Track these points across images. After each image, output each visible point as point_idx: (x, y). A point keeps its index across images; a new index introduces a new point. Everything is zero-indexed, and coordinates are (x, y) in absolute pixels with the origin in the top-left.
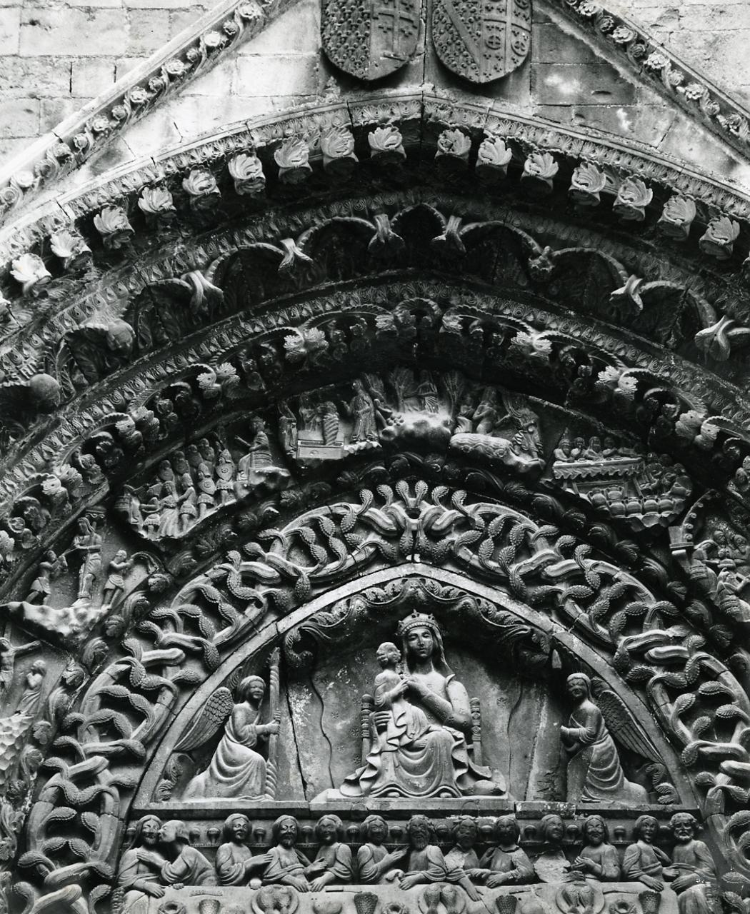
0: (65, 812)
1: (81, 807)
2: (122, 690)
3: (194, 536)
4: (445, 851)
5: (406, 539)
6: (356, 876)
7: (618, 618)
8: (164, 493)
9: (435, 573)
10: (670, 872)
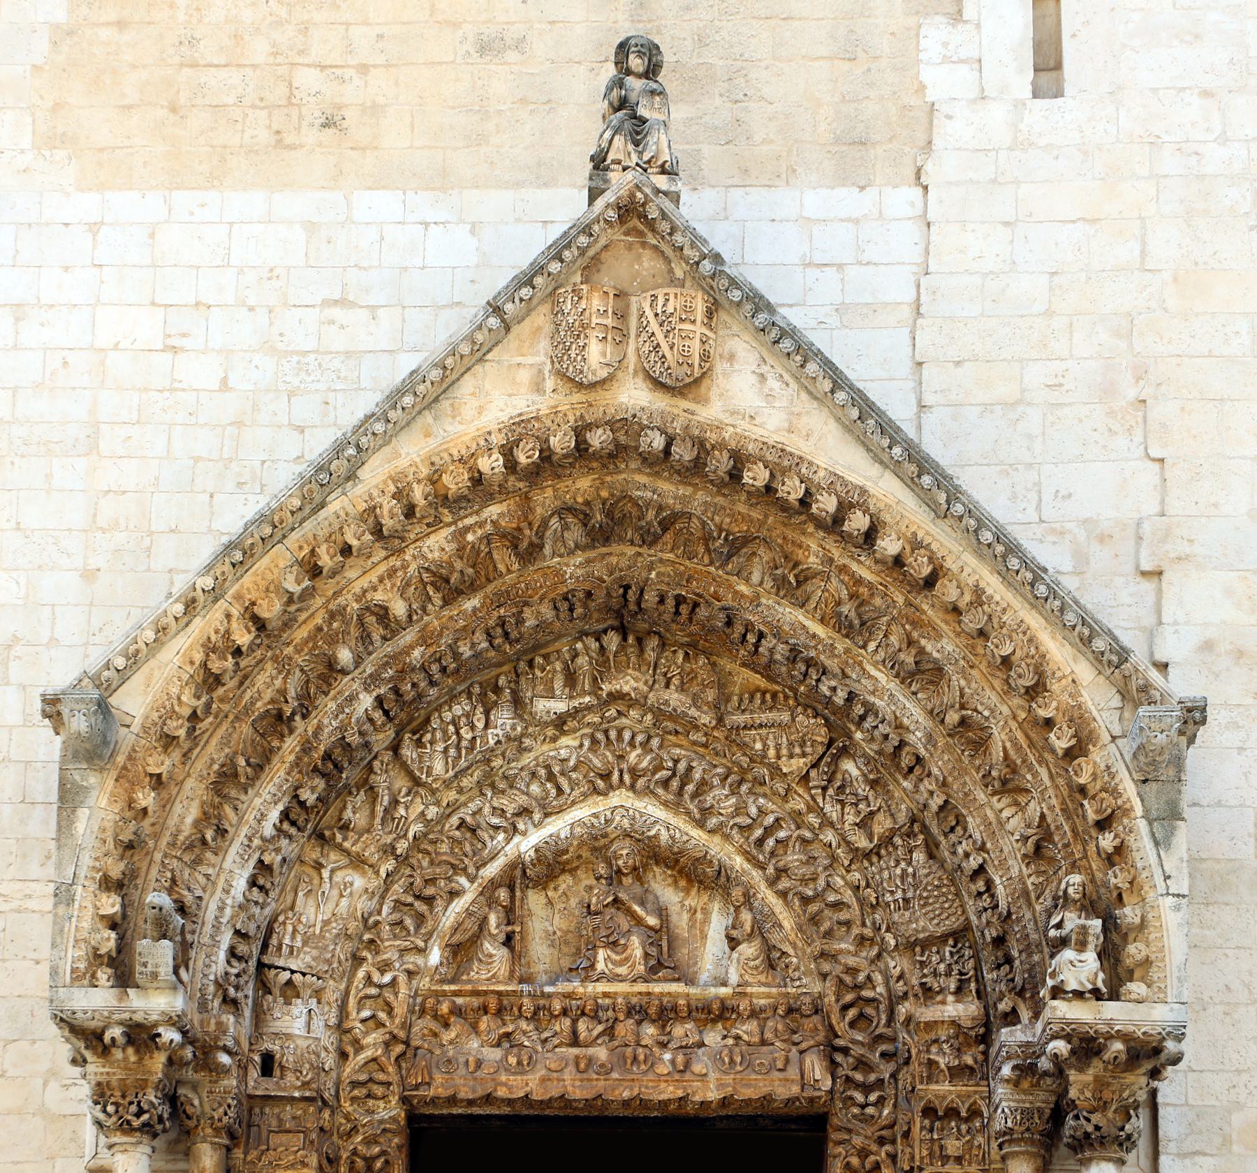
0: (373, 991)
1: (380, 987)
2: (410, 899)
4: (639, 1023)
5: (615, 777)
6: (575, 1041)
8: (432, 743)
10: (796, 1038)
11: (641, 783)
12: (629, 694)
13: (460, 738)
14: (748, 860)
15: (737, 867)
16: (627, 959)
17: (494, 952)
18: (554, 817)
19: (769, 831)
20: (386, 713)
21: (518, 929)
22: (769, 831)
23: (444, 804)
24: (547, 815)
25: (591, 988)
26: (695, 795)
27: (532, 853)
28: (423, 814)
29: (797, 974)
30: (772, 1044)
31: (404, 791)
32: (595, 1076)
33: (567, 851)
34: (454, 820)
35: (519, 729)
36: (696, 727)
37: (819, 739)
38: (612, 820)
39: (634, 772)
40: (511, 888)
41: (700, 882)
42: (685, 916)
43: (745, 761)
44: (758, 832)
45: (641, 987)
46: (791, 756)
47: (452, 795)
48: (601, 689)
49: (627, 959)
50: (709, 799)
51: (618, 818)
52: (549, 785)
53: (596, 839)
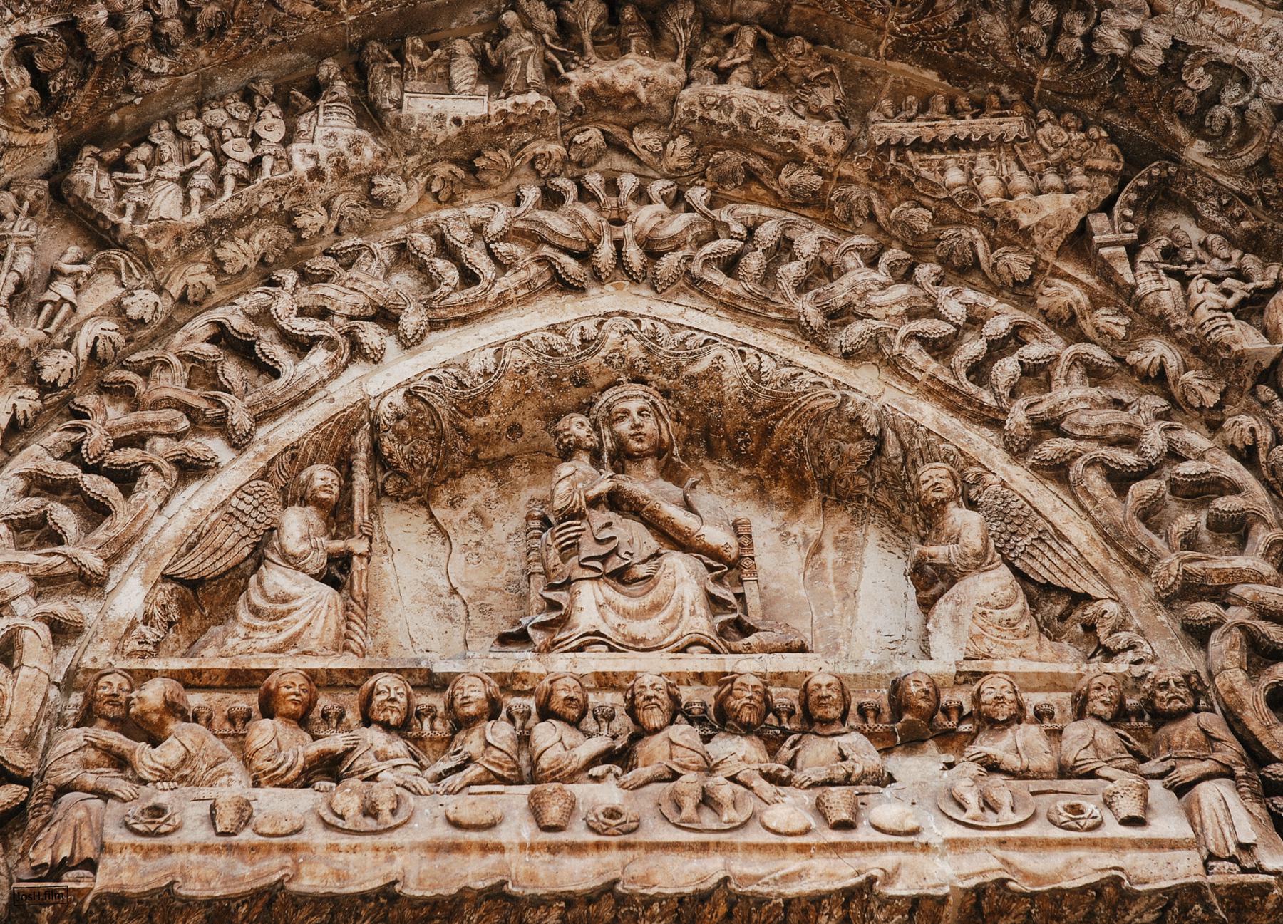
2: (69, 470)
3: (217, 229)
5: (605, 253)
7: (1007, 368)
8: (155, 160)
9: (661, 309)
11: (669, 263)
12: (632, 94)
13: (221, 158)
14: (955, 409)
15: (928, 423)
16: (656, 607)
17: (294, 590)
18: (451, 332)
19: (998, 348)
20: (39, 81)
21: (359, 546)
22: (998, 348)
23: (175, 289)
24: (436, 325)
25: (560, 663)
26: (802, 286)
27: (398, 398)
28: (118, 309)
29: (1123, 636)
30: (1092, 775)
31: (74, 251)
32: (592, 838)
33: (486, 407)
34: (199, 326)
35: (368, 153)
36: (798, 160)
37: (1101, 164)
38: (601, 341)
39: (652, 249)
40: (344, 466)
41: (828, 484)
42: (795, 557)
43: (921, 219)
44: (973, 348)
45: (699, 661)
46: (1038, 192)
47: (197, 275)
48: (567, 82)
49: (656, 607)
50: (840, 291)
51: (614, 337)
52: (440, 264)
53: (556, 384)
